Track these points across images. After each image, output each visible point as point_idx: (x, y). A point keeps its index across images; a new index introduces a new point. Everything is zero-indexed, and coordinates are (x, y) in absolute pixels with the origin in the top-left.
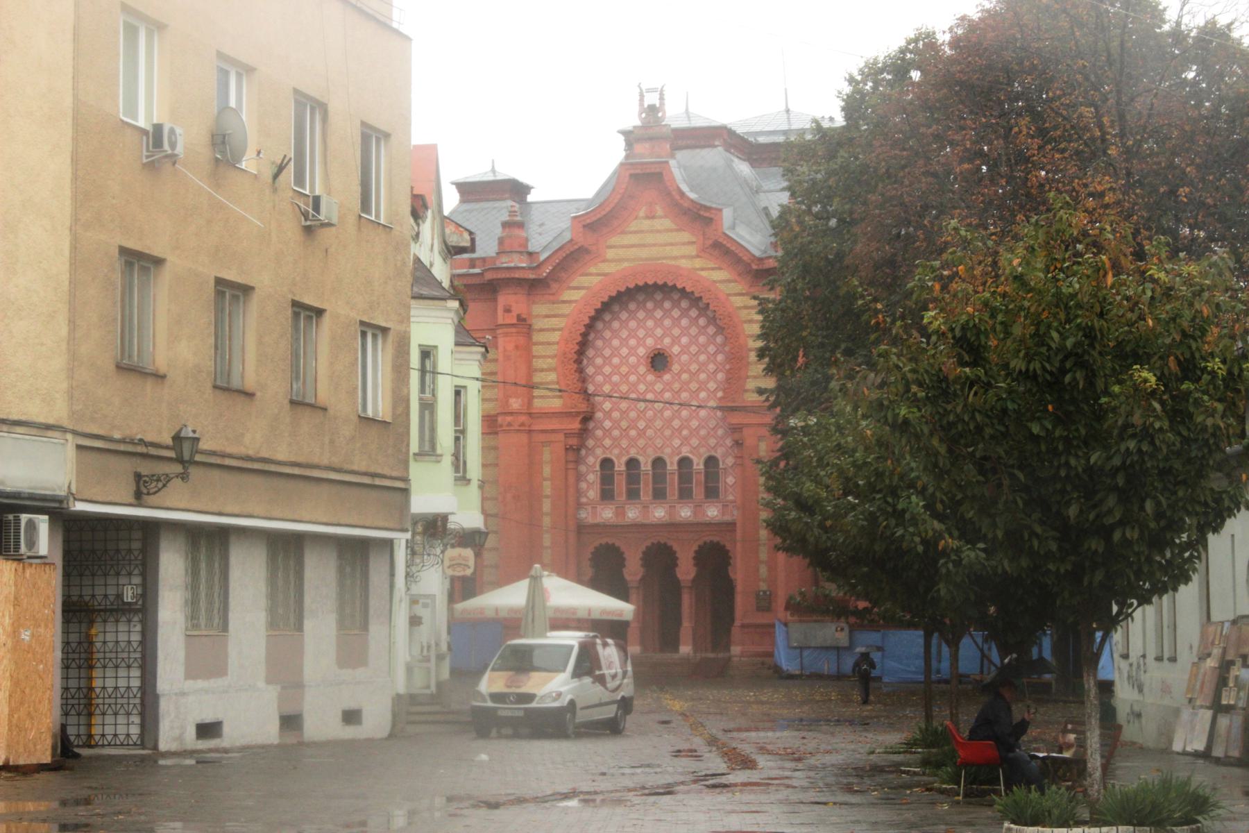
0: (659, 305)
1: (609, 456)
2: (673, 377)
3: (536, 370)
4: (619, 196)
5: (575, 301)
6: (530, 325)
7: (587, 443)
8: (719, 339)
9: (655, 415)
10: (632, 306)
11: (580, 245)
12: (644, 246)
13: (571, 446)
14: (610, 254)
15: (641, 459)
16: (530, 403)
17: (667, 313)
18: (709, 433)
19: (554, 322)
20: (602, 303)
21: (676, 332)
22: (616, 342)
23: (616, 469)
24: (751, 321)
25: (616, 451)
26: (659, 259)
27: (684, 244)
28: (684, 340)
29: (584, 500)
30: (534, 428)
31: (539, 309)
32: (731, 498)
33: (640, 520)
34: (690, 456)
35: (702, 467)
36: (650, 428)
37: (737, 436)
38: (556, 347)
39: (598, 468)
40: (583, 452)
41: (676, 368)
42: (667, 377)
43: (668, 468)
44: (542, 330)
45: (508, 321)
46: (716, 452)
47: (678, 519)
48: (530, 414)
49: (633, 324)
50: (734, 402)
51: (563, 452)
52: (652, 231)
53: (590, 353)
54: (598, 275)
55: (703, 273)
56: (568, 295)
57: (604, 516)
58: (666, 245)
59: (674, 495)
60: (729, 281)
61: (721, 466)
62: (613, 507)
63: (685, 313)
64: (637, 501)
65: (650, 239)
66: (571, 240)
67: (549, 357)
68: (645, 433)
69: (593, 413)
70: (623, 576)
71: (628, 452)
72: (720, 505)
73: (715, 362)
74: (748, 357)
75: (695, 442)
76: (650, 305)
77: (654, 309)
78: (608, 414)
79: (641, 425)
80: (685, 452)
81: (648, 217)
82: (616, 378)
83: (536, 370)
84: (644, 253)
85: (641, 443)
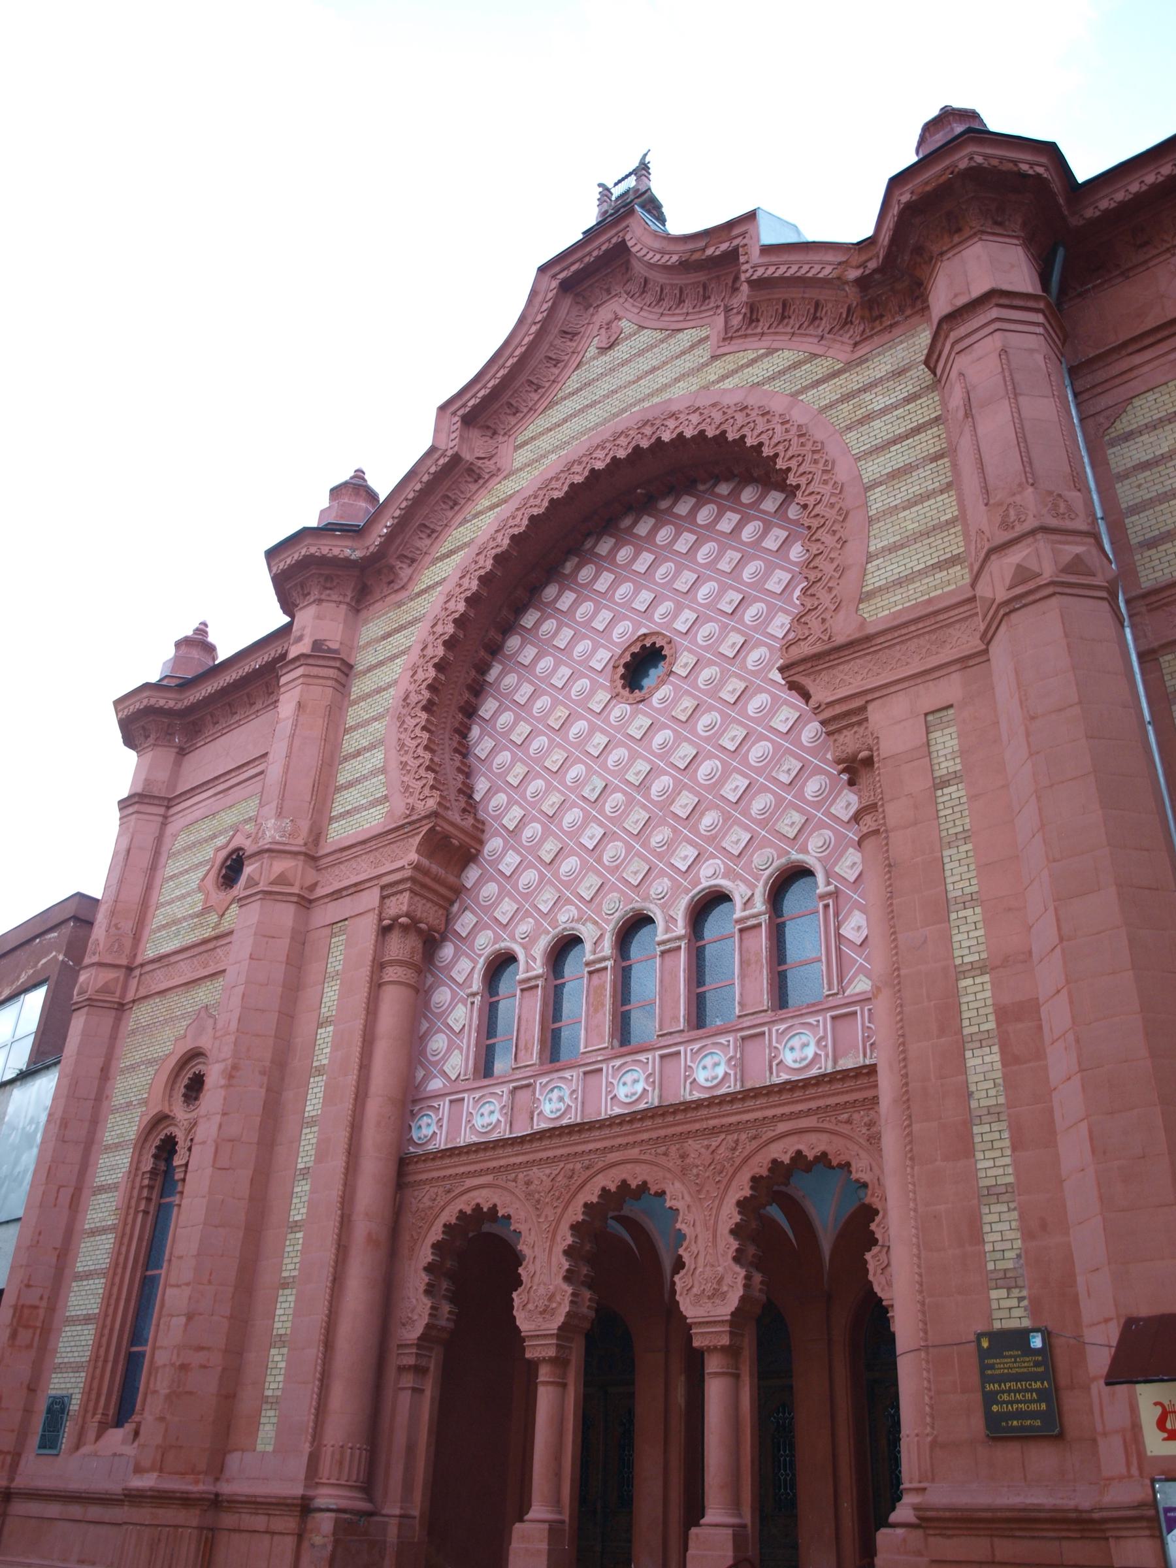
0: (646, 543)
1: (506, 944)
2: (676, 688)
4: (534, 329)
6: (351, 667)
7: (458, 927)
8: (796, 552)
9: (630, 801)
11: (450, 453)
12: (593, 404)
13: (395, 919)
14: (521, 457)
15: (588, 933)
16: (317, 835)
18: (780, 800)
19: (400, 640)
25: (525, 927)
26: (624, 410)
27: (683, 353)
30: (320, 892)
31: (373, 628)
32: (861, 985)
34: (725, 883)
37: (850, 741)
39: (477, 984)
40: (447, 951)
41: (683, 663)
46: (804, 850)
52: (612, 370)
53: (488, 707)
55: (728, 384)
58: (640, 378)
59: (676, 1018)
60: (796, 365)
62: (506, 1089)
63: (706, 533)
65: (604, 387)
66: (432, 450)
67: (375, 719)
68: (599, 860)
69: (481, 843)
71: (554, 923)
72: (823, 1021)
75: (736, 839)
80: (709, 876)
81: (603, 350)
84: (594, 417)
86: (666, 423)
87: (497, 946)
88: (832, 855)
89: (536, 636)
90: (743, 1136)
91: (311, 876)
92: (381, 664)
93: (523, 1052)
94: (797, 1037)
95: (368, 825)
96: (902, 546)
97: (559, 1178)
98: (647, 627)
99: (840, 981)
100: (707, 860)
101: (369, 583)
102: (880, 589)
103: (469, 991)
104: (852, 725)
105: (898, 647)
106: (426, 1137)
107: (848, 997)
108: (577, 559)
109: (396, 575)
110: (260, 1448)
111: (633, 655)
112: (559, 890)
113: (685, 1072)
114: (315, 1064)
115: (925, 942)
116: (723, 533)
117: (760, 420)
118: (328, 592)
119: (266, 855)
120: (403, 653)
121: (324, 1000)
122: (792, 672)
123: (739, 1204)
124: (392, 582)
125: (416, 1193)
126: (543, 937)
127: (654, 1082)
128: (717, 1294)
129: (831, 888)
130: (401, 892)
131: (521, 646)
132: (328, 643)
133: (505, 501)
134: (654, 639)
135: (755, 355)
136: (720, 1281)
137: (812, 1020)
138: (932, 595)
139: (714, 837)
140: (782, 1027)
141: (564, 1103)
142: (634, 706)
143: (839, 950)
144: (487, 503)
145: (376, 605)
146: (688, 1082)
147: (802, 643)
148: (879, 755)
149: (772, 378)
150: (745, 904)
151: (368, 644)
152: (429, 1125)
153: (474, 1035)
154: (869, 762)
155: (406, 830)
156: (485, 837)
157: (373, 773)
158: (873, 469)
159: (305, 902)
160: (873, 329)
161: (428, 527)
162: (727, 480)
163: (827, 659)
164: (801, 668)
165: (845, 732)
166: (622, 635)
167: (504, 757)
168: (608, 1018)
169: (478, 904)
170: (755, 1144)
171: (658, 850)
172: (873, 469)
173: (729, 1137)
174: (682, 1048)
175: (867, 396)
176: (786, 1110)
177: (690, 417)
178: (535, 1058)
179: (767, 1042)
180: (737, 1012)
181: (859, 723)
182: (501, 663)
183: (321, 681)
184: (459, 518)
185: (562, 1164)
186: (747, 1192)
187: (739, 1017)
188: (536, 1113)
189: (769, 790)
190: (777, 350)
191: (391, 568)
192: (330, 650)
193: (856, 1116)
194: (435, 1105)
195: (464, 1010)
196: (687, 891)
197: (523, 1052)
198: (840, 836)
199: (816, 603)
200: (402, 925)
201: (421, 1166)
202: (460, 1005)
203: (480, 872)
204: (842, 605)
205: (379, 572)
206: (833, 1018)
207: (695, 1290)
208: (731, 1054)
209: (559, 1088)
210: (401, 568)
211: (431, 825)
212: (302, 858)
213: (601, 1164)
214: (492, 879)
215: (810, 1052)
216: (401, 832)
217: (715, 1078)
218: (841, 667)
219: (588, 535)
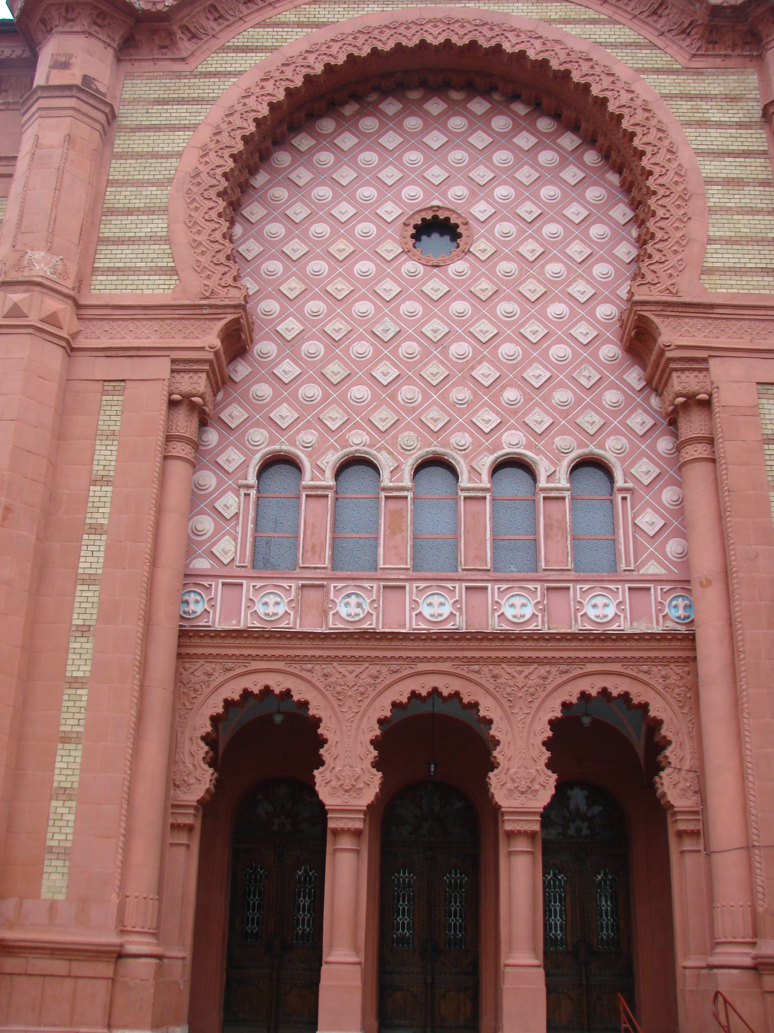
3: (112, 212)
5: (240, 73)
6: (114, 117)
7: (224, 416)
9: (426, 353)
10: (369, 124)
13: (187, 397)
15: (384, 461)
16: (81, 282)
17: (456, 140)
18: (579, 401)
20: (307, 77)
21: (481, 174)
22: (323, 192)
23: (307, 481)
24: (703, 124)
25: (310, 437)
28: (502, 191)
29: (202, 564)
30: (81, 343)
32: (652, 569)
33: (375, 624)
35: (564, 483)
36: (409, 381)
38: (174, 162)
39: (252, 479)
40: (212, 437)
41: (481, 247)
42: (459, 266)
43: (464, 482)
44: (140, 128)
45: (54, 82)
47: (495, 625)
48: (75, 301)
49: (369, 157)
50: (676, 294)
51: (164, 407)
53: (254, 211)
54: (300, 25)
56: (215, 62)
57: (261, 610)
60: (637, 46)
61: (620, 482)
63: (502, 140)
64: (372, 574)
68: (393, 397)
70: (316, 794)
73: (586, 239)
74: (703, 195)
75: (539, 419)
76: (413, 123)
77: (426, 130)
78: (289, 346)
79: (385, 372)
82: (318, 266)
83: (112, 212)
85: (383, 417)
86: (506, 34)
87: (277, 447)
88: (630, 457)
89: (310, 161)
90: (554, 670)
91: (76, 326)
92: (156, 128)
93: (309, 554)
94: (600, 597)
95: (150, 292)
96: (736, 243)
97: (362, 676)
98: (441, 201)
99: (635, 561)
100: (508, 429)
101: (138, 37)
102: (718, 270)
103: (244, 482)
104: (694, 370)
105: (734, 322)
106: (194, 612)
107: (642, 575)
108: (358, 106)
109: (174, 43)
110: (45, 894)
111: (423, 220)
112: (348, 413)
113: (493, 606)
114: (88, 521)
115: (757, 556)
116: (520, 149)
117: (603, 76)
118: (97, 28)
119: (37, 289)
120: (186, 128)
121: (96, 457)
122: (645, 308)
123: (551, 722)
124: (166, 47)
125: (188, 665)
126: (331, 451)
127: (460, 609)
128: (529, 791)
129: (630, 485)
130: (196, 371)
131: (291, 165)
132: (96, 83)
133: (318, 25)
134: (447, 214)
135: (597, 17)
136: (532, 782)
137: (612, 587)
138: (762, 292)
139: (516, 412)
140: (586, 587)
141: (363, 610)
142: (428, 268)
143: (634, 537)
144: (293, 19)
145: (144, 64)
146: (497, 614)
147: (652, 287)
148: (718, 402)
149: (614, 46)
150: (548, 477)
151: (136, 101)
152: (197, 602)
153: (250, 526)
154: (707, 404)
155: (204, 311)
156: (256, 337)
157: (153, 239)
158: (711, 168)
159: (71, 350)
160: (707, 50)
161: (217, 11)
162: (527, 103)
163: (676, 309)
164: (654, 308)
165: (687, 373)
166: (413, 198)
167: (276, 266)
168: (410, 543)
169: (248, 401)
170: (565, 677)
171: (458, 406)
172: (711, 168)
173: (541, 667)
174: (489, 585)
175: (704, 105)
176: (597, 654)
177: (533, 41)
178: (327, 563)
179: (572, 596)
180: (543, 567)
181: (700, 370)
182: (269, 174)
183: (88, 120)
184: (257, 18)
185: (366, 665)
186: (559, 714)
187: (545, 570)
188: (331, 613)
189: (568, 387)
190: (619, 23)
191: (171, 34)
192: (97, 91)
193: (654, 668)
194: (206, 584)
195: (237, 499)
196: (492, 452)
197: (309, 554)
198: (634, 447)
199: (663, 259)
200: (193, 406)
201: (195, 640)
202: (230, 493)
203: (250, 370)
204: (686, 269)
205: (154, 32)
206: (630, 589)
207: (509, 785)
208: (539, 599)
209: (358, 595)
210: (181, 38)
211: (236, 316)
212: (70, 302)
213: (409, 671)
214: (263, 380)
215: (611, 612)
216: (198, 312)
217: (522, 616)
218: (687, 320)
219: (374, 89)
